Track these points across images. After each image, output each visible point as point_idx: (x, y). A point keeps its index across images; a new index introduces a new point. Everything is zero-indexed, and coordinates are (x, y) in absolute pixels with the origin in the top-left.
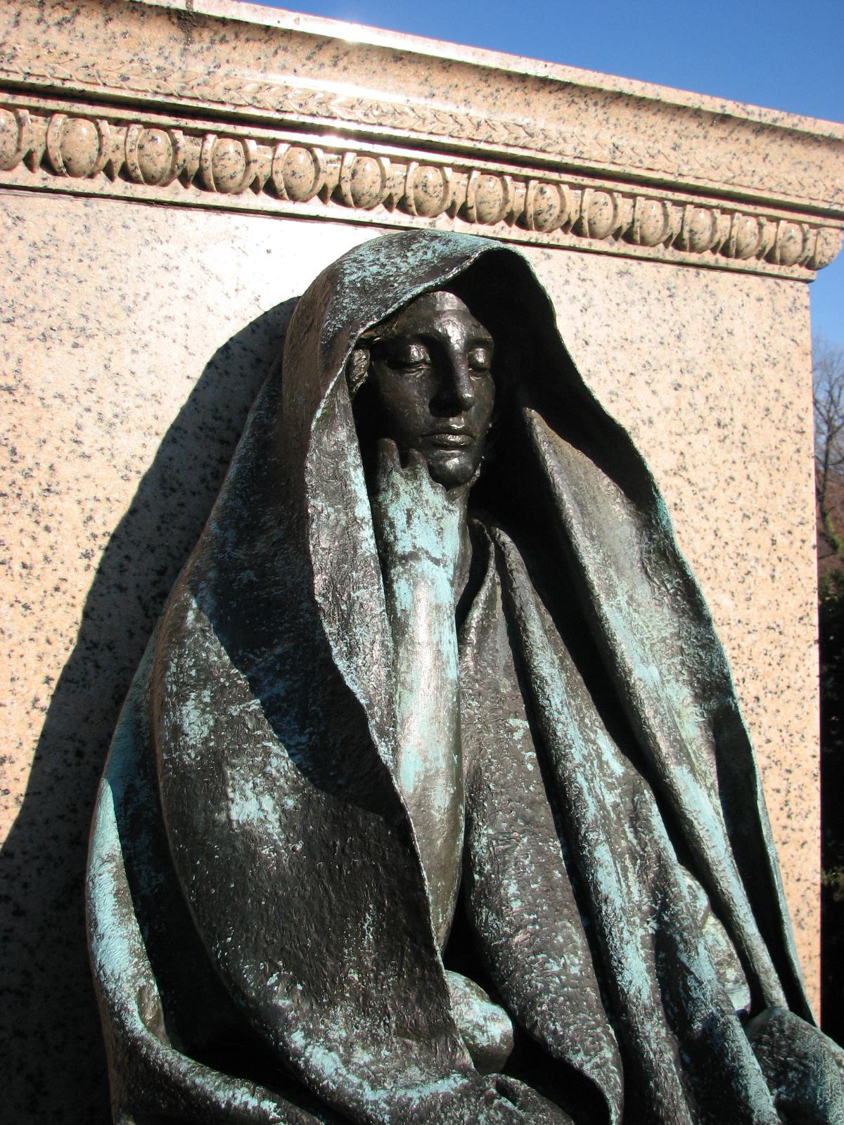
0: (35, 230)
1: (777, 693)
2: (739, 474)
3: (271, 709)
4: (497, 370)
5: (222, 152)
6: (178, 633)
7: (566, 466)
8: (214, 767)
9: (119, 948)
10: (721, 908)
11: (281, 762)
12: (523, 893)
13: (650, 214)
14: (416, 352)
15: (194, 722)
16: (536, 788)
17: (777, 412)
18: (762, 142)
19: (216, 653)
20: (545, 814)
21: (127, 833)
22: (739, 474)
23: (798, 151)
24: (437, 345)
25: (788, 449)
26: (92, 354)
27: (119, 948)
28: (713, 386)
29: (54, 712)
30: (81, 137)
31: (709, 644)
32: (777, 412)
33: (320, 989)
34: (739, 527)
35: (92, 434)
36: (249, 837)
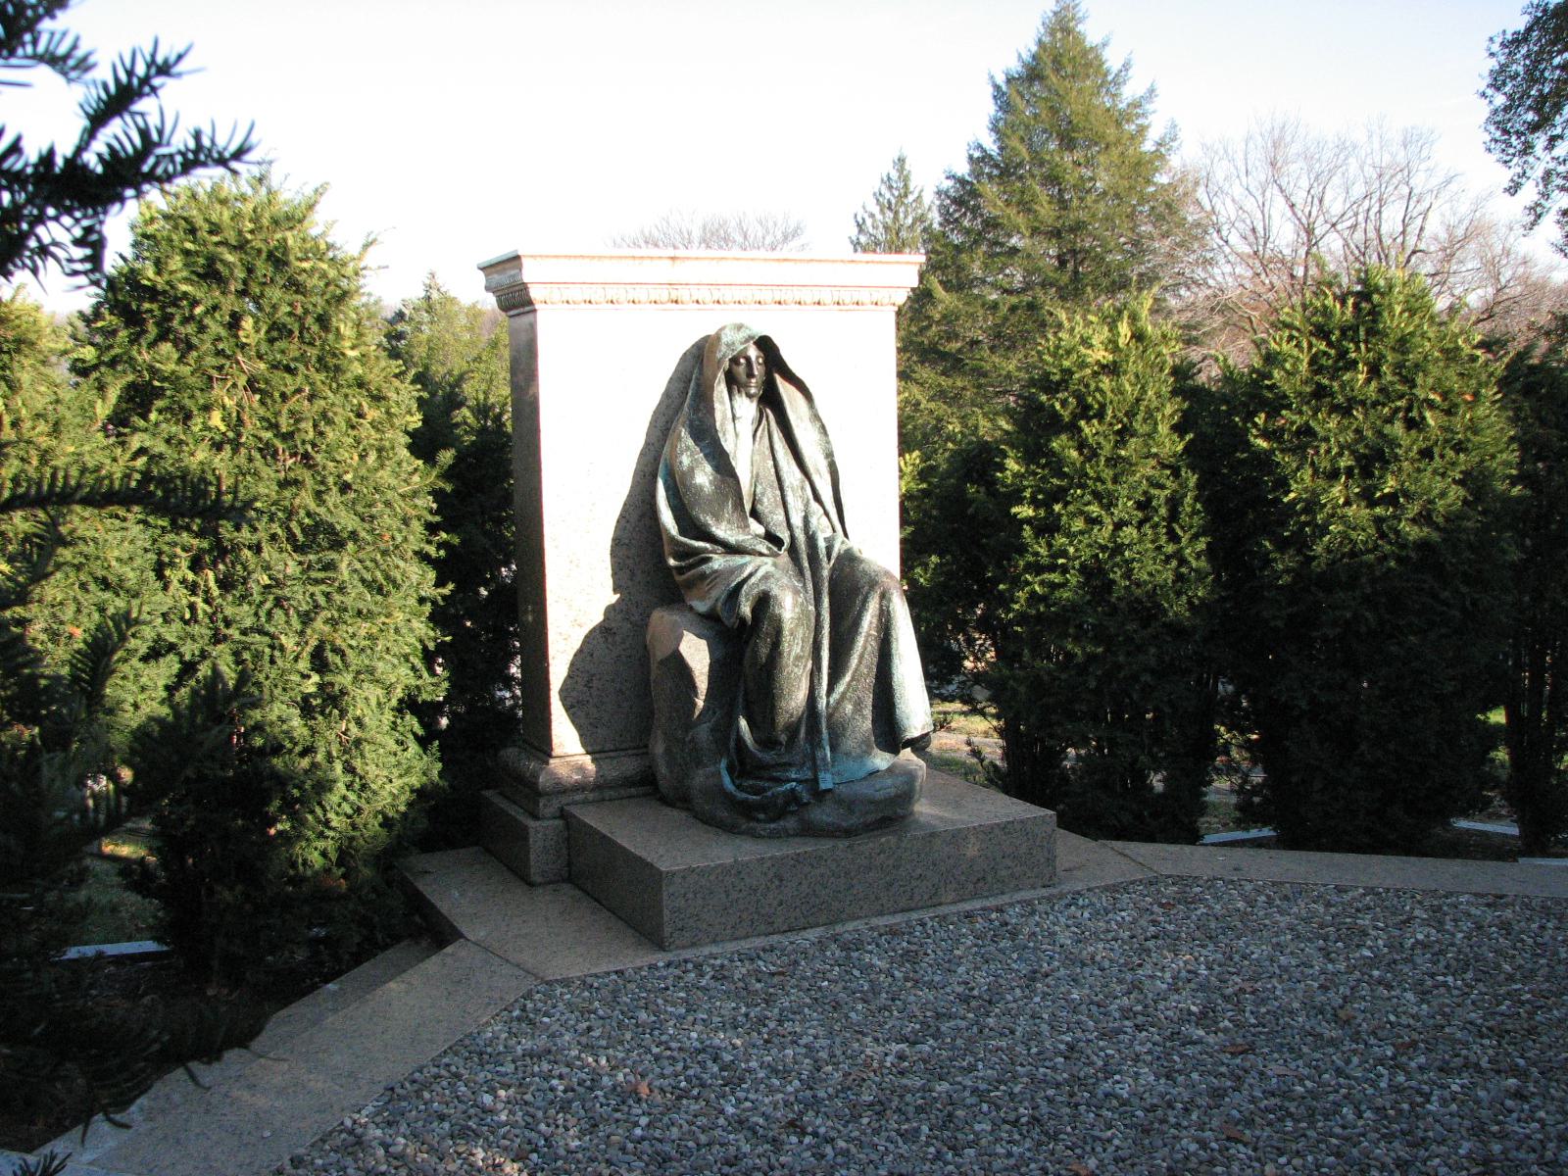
3: (706, 456)
4: (766, 362)
6: (679, 438)
7: (785, 389)
8: (692, 470)
9: (667, 518)
10: (827, 514)
11: (708, 468)
12: (769, 503)
14: (742, 361)
15: (686, 460)
16: (774, 478)
19: (690, 442)
20: (776, 484)
21: (667, 490)
24: (748, 359)
27: (667, 518)
29: (638, 463)
31: (828, 442)
33: (718, 518)
36: (701, 488)
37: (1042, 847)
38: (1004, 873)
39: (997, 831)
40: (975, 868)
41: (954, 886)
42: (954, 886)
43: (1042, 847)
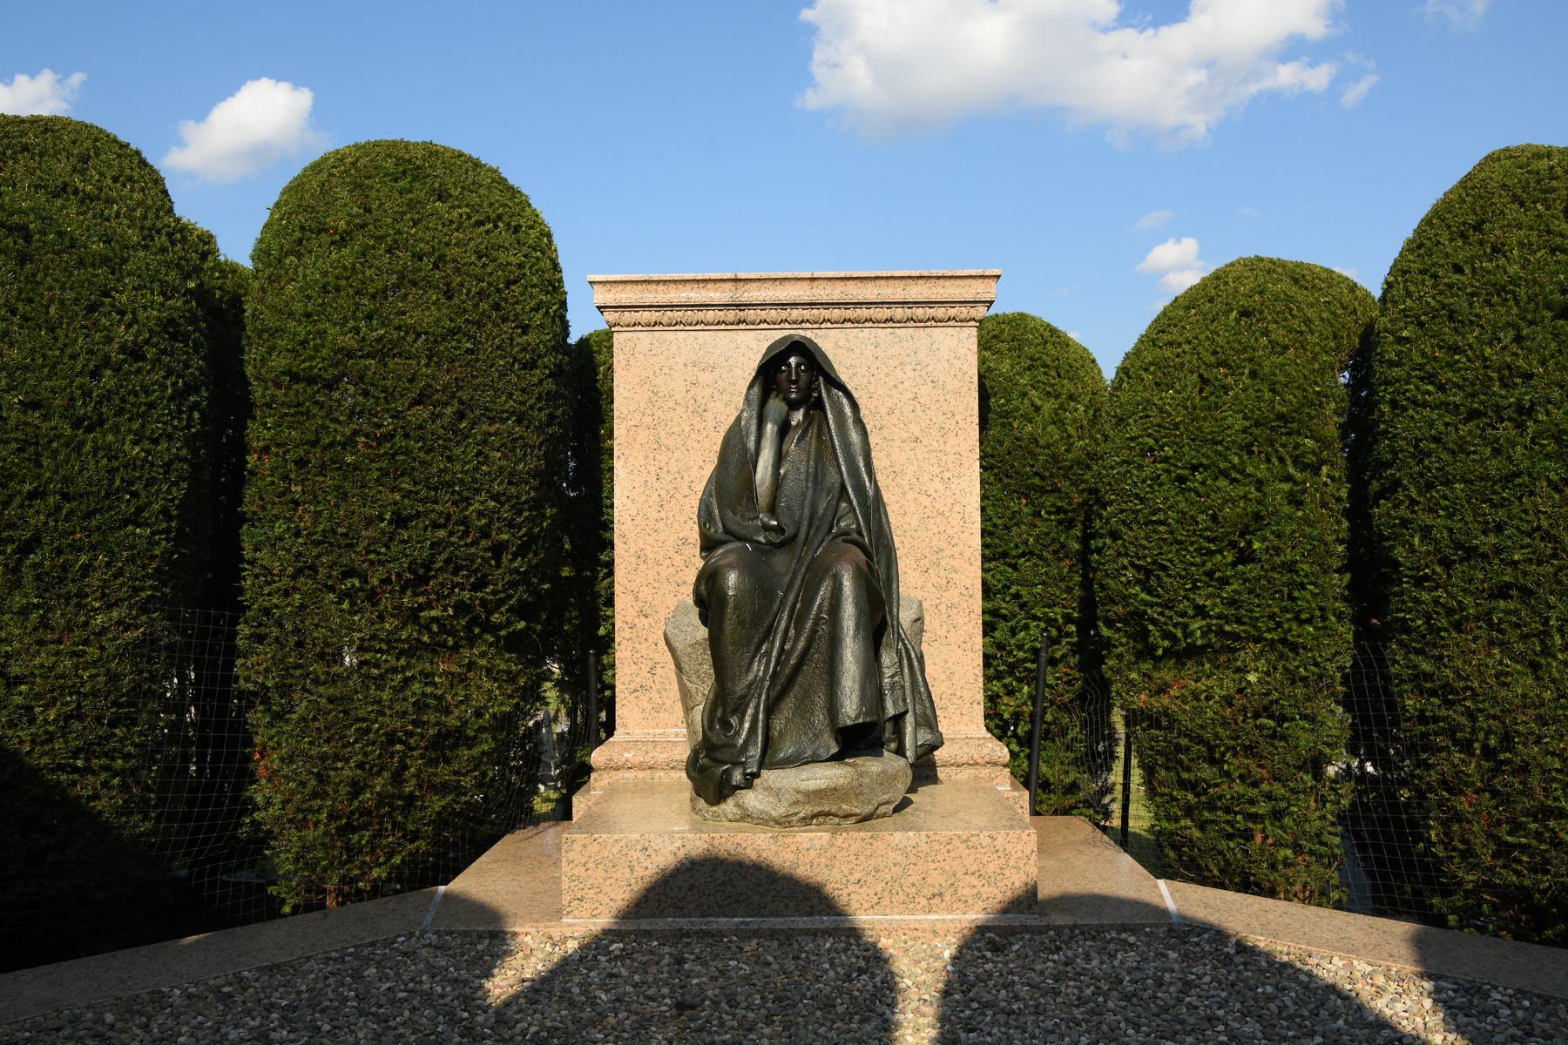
0: (701, 341)
1: (959, 477)
2: (941, 398)
5: (751, 314)
13: (899, 313)
17: (960, 375)
18: (941, 282)
22: (941, 398)
23: (958, 282)
25: (965, 389)
26: (716, 373)
28: (930, 369)
30: (710, 315)
32: (960, 375)
34: (942, 418)
35: (716, 394)
37: (1018, 868)
38: (966, 891)
39: (957, 843)
40: (929, 880)
41: (902, 897)
42: (902, 897)
43: (1018, 868)
